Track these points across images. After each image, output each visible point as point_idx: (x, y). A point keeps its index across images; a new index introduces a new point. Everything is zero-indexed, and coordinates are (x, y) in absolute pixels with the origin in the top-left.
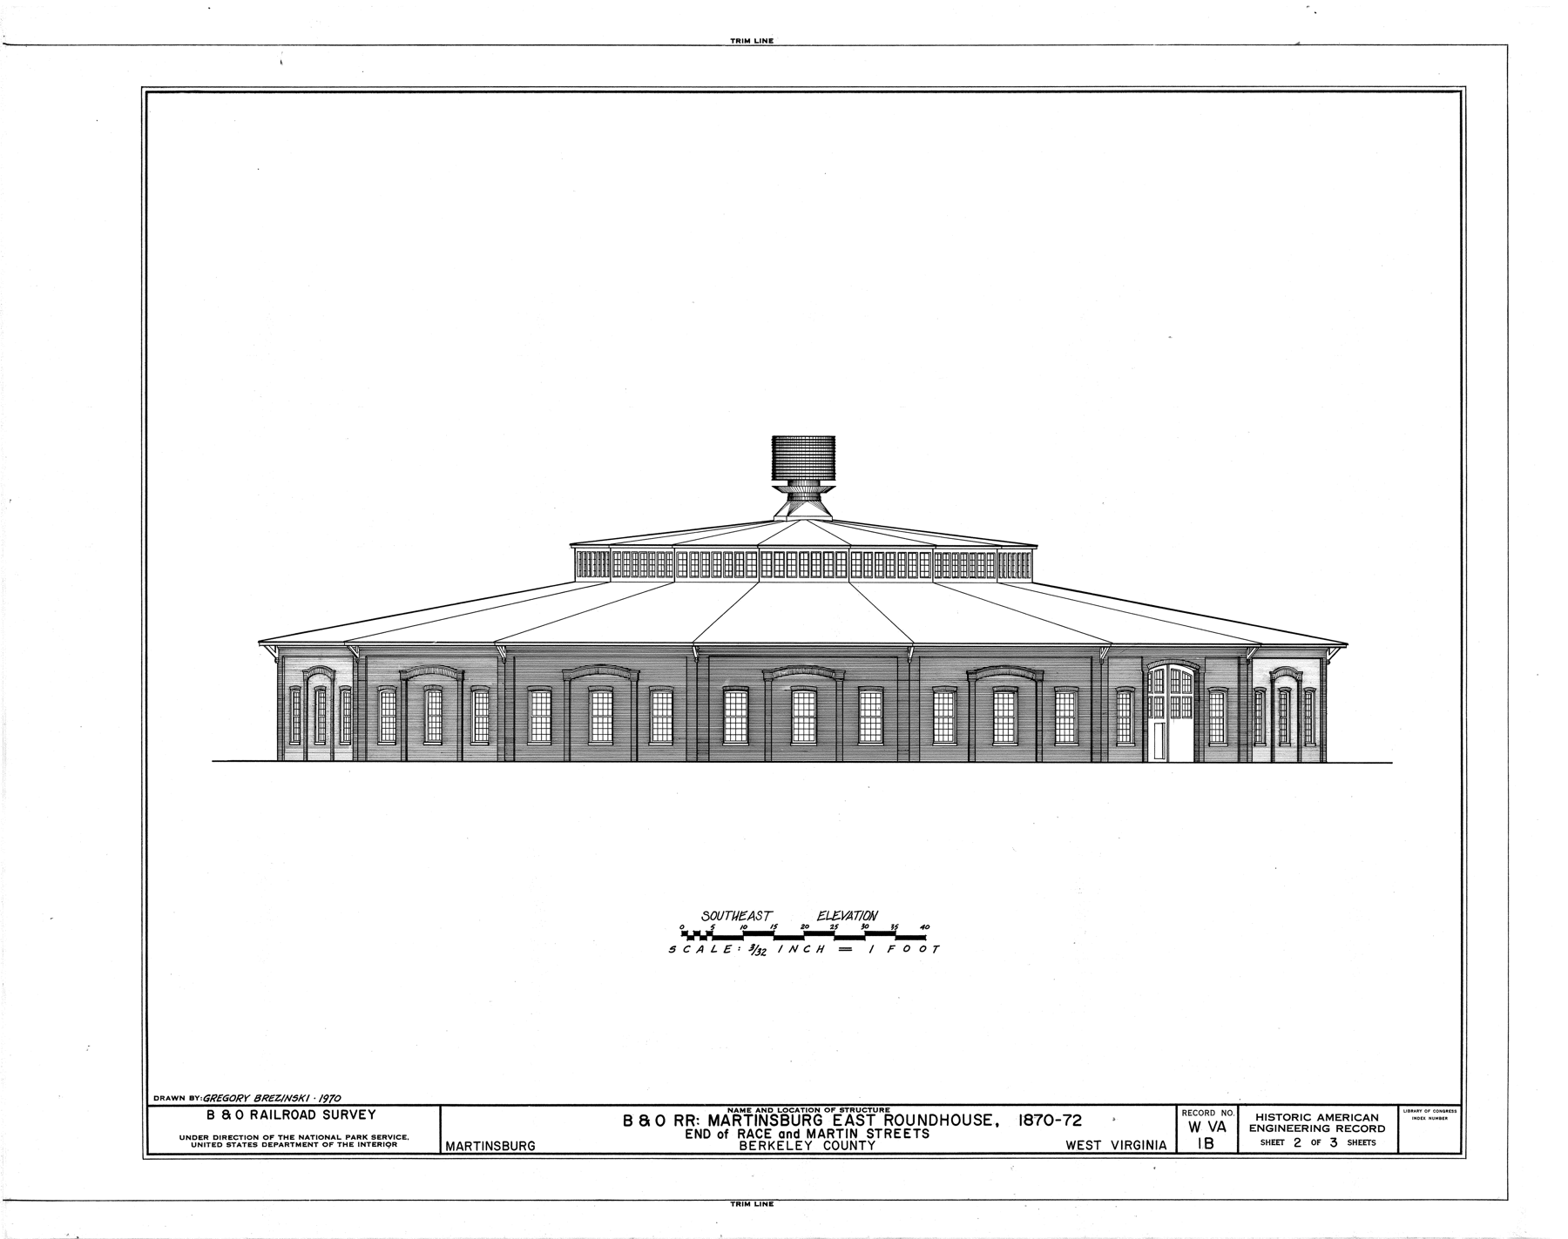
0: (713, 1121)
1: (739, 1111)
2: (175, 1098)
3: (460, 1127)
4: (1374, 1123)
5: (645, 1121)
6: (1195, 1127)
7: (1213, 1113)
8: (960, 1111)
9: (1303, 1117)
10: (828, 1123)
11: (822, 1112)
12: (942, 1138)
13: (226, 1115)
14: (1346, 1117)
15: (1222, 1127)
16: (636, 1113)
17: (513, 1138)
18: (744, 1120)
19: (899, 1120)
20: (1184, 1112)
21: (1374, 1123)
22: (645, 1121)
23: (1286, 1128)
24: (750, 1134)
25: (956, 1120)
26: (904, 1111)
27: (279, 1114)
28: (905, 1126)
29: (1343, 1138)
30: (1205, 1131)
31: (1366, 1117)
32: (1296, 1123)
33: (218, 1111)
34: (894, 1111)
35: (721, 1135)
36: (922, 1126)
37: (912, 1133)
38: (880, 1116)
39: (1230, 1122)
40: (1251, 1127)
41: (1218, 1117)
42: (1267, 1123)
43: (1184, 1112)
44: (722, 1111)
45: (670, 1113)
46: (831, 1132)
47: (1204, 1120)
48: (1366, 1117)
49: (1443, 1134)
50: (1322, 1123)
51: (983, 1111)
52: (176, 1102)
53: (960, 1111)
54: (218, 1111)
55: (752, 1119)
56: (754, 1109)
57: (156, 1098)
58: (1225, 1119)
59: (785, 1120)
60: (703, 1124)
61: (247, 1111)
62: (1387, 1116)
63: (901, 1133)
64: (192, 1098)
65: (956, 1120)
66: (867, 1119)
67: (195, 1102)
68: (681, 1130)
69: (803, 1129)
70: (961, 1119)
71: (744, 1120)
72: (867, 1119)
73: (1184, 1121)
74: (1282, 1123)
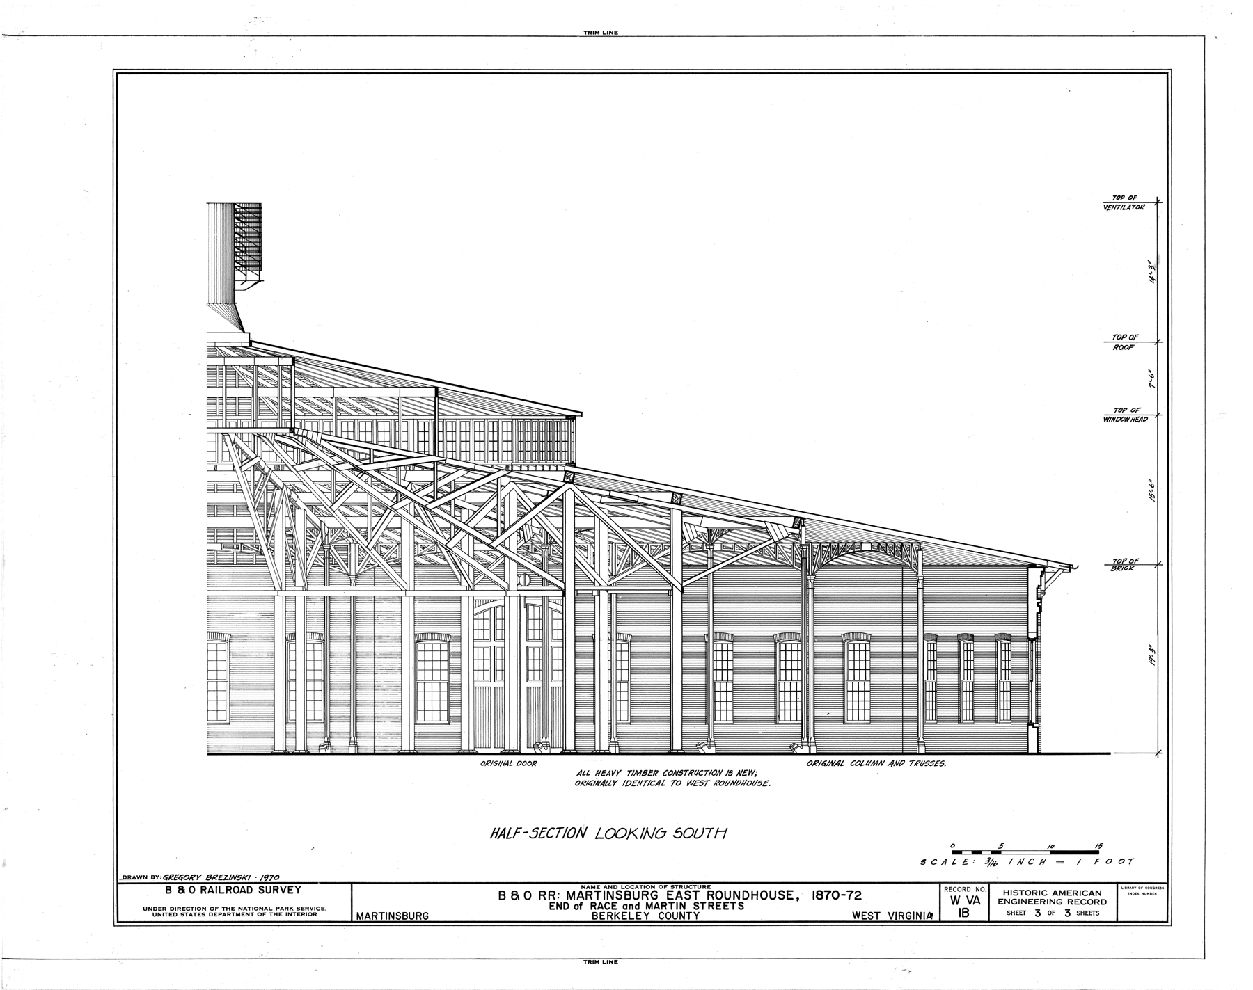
0: (570, 895)
1: (590, 888)
4: (1098, 897)
5: (515, 895)
7: (969, 890)
8: (767, 887)
9: (1041, 893)
10: (662, 897)
14: (1075, 892)
16: (508, 889)
18: (595, 895)
19: (719, 895)
20: (946, 889)
21: (1098, 897)
22: (515, 895)
24: (601, 906)
28: (723, 900)
31: (1092, 893)
34: (714, 888)
37: (730, 906)
38: (703, 895)
39: (983, 897)
41: (973, 893)
44: (577, 888)
46: (664, 905)
47: (963, 895)
48: (1092, 893)
50: (1056, 897)
51: (785, 887)
53: (767, 887)
55: (601, 894)
56: (602, 886)
59: (628, 895)
60: (562, 898)
63: (721, 906)
65: (764, 895)
66: (693, 894)
69: (643, 903)
70: (768, 894)
71: (595, 895)
72: (693, 894)
73: (946, 897)
74: (1024, 897)
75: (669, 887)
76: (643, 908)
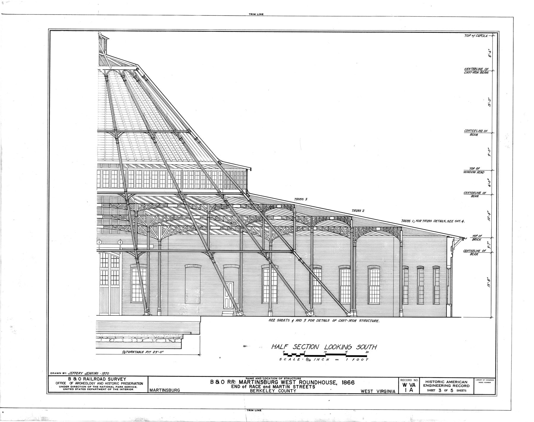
0: (241, 382)
1: (249, 379)
2: (58, 373)
3: (155, 384)
4: (466, 384)
5: (217, 382)
6: (405, 385)
7: (411, 380)
8: (325, 379)
9: (442, 382)
10: (280, 383)
11: (278, 379)
13: (75, 379)
14: (456, 382)
15: (414, 385)
16: (215, 379)
17: (173, 387)
18: (251, 382)
19: (304, 382)
20: (401, 380)
21: (466, 384)
22: (217, 382)
23: (437, 386)
24: (254, 386)
25: (323, 382)
26: (306, 379)
27: (93, 379)
28: (306, 384)
31: (463, 382)
32: (439, 384)
33: (72, 378)
34: (302, 379)
36: (312, 385)
37: (309, 387)
38: (297, 382)
39: (417, 383)
40: (424, 386)
41: (413, 382)
43: (401, 380)
44: (244, 379)
45: (226, 379)
46: (280, 386)
47: (408, 382)
48: (463, 382)
50: (448, 384)
51: (333, 379)
52: (58, 374)
53: (325, 379)
54: (72, 378)
55: (254, 382)
56: (255, 378)
58: (415, 382)
59: (265, 382)
60: (237, 383)
61: (82, 378)
62: (470, 382)
63: (305, 387)
64: (63, 373)
65: (323, 382)
66: (293, 382)
67: (64, 375)
68: (230, 385)
69: (272, 385)
70: (325, 382)
71: (251, 382)
72: (293, 382)
73: (401, 383)
74: (435, 384)
75: (283, 379)
76: (272, 387)
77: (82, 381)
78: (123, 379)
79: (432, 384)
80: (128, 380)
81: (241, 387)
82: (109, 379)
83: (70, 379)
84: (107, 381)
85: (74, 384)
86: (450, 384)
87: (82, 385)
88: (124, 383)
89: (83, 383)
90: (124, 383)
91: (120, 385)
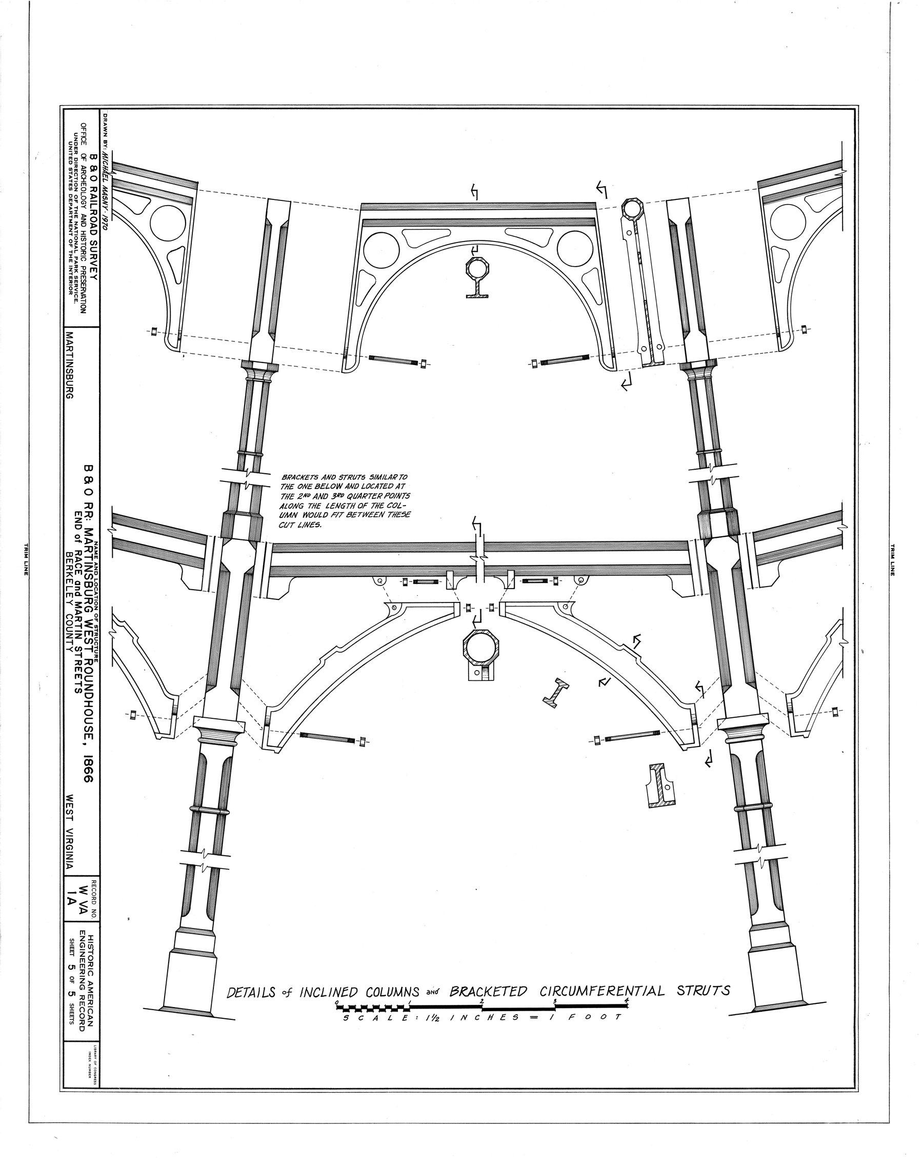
0: (89, 531)
2: (105, 129)
3: (84, 342)
4: (87, 1023)
5: (88, 480)
6: (83, 890)
7: (94, 903)
8: (96, 716)
9: (91, 971)
11: (95, 612)
12: (76, 703)
13: (93, 169)
14: (91, 1002)
16: (94, 474)
17: (75, 383)
18: (89, 554)
19: (89, 670)
20: (94, 881)
21: (87, 1023)
22: (88, 480)
24: (78, 560)
25: (89, 713)
27: (94, 207)
28: (84, 675)
29: (76, 1000)
30: (80, 898)
32: (86, 965)
33: (96, 162)
35: (77, 537)
36: (84, 687)
37: (78, 680)
38: (91, 655)
39: (87, 916)
40: (83, 931)
42: (86, 943)
43: (94, 881)
44: (95, 538)
45: (94, 499)
46: (79, 619)
47: (88, 897)
49: (78, 1075)
50: (86, 984)
51: (96, 732)
52: (103, 130)
53: (96, 716)
54: (96, 162)
55: (89, 560)
56: (97, 561)
57: (105, 115)
59: (88, 585)
60: (86, 524)
61: (96, 184)
62: (91, 1033)
63: (78, 672)
64: (105, 142)
66: (89, 646)
67: (102, 144)
71: (89, 554)
72: (89, 646)
73: (87, 882)
74: (87, 955)
76: (77, 599)
77: (90, 184)
78: (93, 273)
79: (87, 950)
80: (92, 285)
81: (78, 532)
82: (93, 243)
83: (93, 157)
84: (90, 238)
85: (81, 162)
86: (87, 989)
87: (80, 181)
88: (84, 273)
89: (84, 183)
90: (84, 273)
91: (80, 264)
